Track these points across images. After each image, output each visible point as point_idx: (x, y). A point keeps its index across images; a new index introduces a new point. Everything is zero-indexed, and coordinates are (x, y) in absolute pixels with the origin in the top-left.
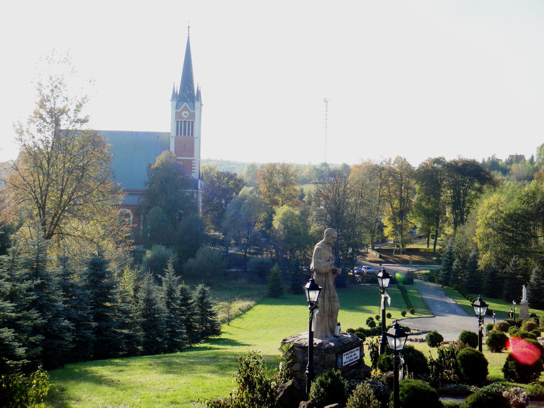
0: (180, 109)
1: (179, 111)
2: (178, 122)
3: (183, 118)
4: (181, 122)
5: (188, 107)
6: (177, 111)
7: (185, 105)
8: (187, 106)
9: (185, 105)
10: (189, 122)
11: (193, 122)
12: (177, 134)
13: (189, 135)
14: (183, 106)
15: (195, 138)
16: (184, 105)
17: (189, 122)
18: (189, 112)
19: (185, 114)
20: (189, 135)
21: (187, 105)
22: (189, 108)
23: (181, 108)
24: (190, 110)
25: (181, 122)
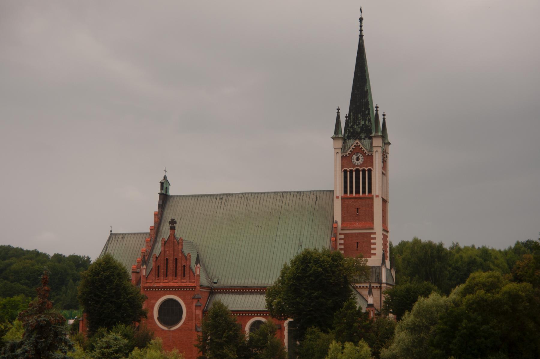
0: (349, 152)
1: (347, 154)
2: (345, 172)
3: (354, 166)
4: (351, 172)
6: (345, 154)
7: (357, 143)
8: (359, 146)
9: (357, 143)
10: (364, 171)
11: (370, 171)
12: (345, 192)
13: (364, 192)
15: (374, 196)
17: (364, 171)
19: (358, 159)
20: (364, 192)
21: (359, 144)
25: (351, 172)
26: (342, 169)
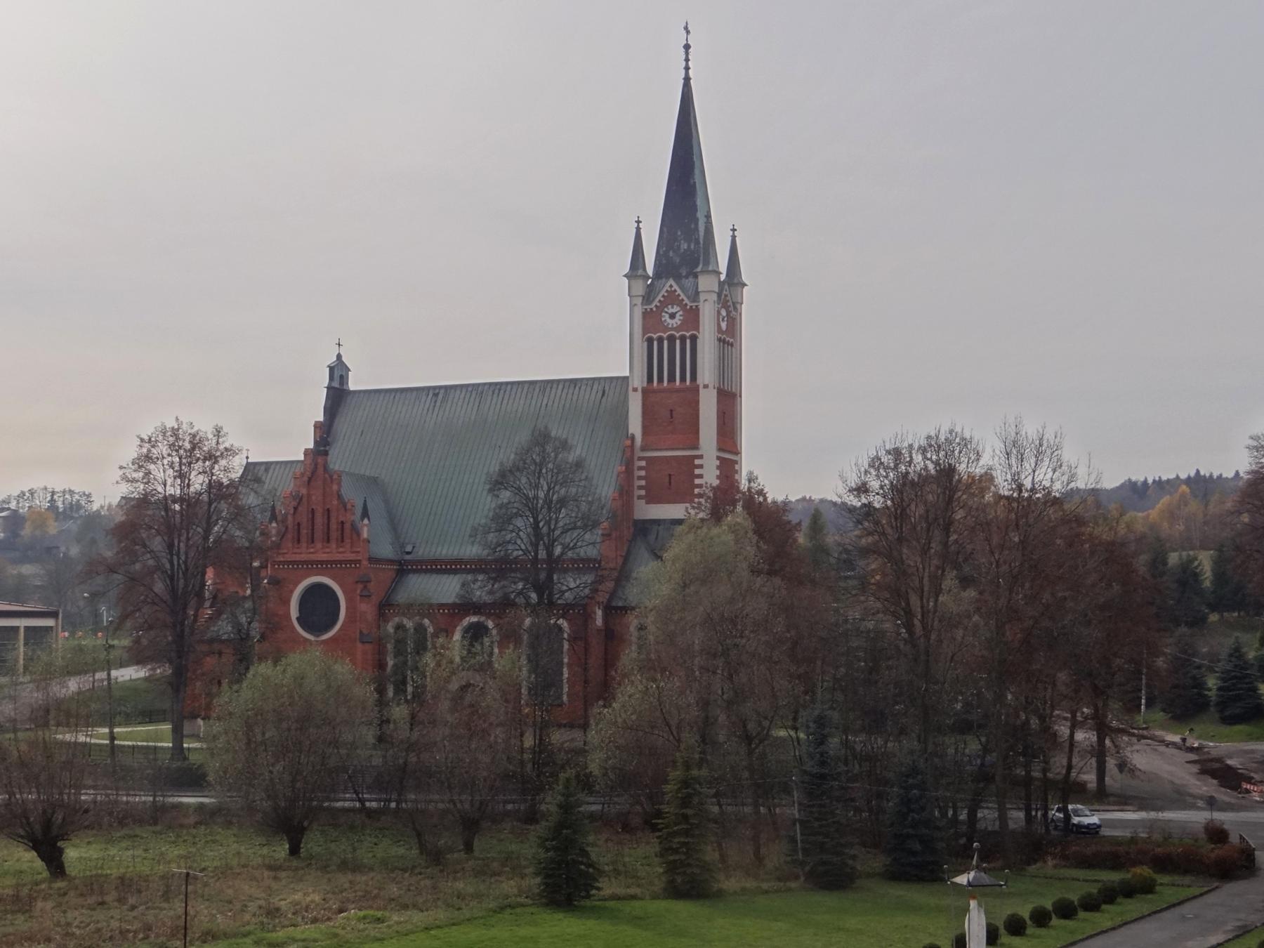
0: (656, 302)
1: (653, 306)
2: (650, 341)
3: (666, 329)
4: (660, 340)
5: (679, 291)
6: (648, 307)
7: (671, 286)
8: (675, 291)
9: (671, 286)
10: (683, 339)
11: (694, 339)
13: (683, 379)
14: (663, 292)
15: (701, 386)
16: (667, 287)
17: (683, 339)
18: (683, 307)
19: (672, 316)
20: (683, 379)
21: (675, 287)
22: (682, 296)
23: (660, 297)
24: (686, 301)
25: (660, 340)
26: (643, 336)
